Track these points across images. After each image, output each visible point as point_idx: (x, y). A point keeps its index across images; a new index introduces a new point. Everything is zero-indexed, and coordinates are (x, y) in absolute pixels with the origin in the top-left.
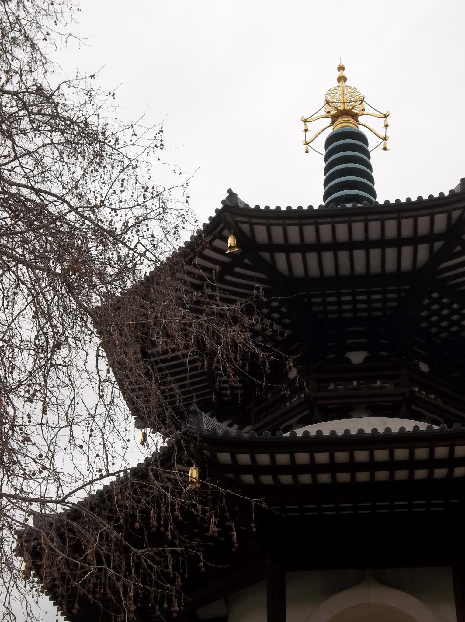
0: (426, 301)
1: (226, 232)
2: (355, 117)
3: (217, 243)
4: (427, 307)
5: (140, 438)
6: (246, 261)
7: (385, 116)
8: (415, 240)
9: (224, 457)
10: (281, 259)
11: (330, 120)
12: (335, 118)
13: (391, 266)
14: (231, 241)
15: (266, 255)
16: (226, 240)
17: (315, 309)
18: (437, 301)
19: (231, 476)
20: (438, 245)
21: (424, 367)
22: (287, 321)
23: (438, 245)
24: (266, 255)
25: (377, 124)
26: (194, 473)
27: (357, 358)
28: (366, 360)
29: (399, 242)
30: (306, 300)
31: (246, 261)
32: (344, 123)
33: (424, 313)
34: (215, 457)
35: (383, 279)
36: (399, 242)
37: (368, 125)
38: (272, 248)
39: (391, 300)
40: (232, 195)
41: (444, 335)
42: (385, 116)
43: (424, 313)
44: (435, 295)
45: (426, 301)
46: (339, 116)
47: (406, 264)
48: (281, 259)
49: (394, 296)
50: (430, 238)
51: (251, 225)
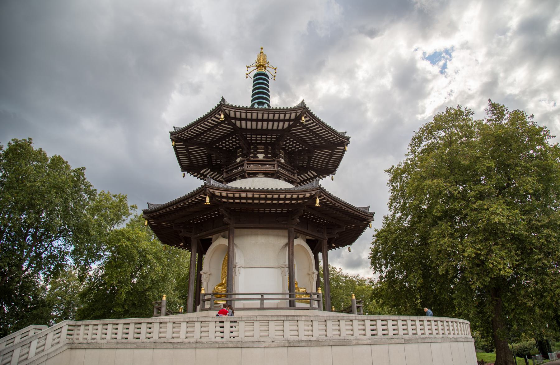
1: (220, 112)
2: (265, 67)
3: (217, 116)
4: (285, 141)
5: (183, 175)
8: (284, 121)
9: (218, 193)
11: (256, 68)
12: (258, 67)
13: (275, 128)
14: (222, 116)
15: (233, 121)
16: (220, 115)
18: (289, 139)
20: (291, 123)
21: (283, 161)
22: (238, 142)
23: (291, 123)
24: (233, 121)
25: (273, 71)
26: (208, 199)
28: (264, 157)
29: (279, 121)
32: (262, 70)
36: (279, 121)
37: (269, 71)
38: (235, 118)
40: (223, 100)
48: (238, 123)
50: (289, 120)
51: (229, 111)
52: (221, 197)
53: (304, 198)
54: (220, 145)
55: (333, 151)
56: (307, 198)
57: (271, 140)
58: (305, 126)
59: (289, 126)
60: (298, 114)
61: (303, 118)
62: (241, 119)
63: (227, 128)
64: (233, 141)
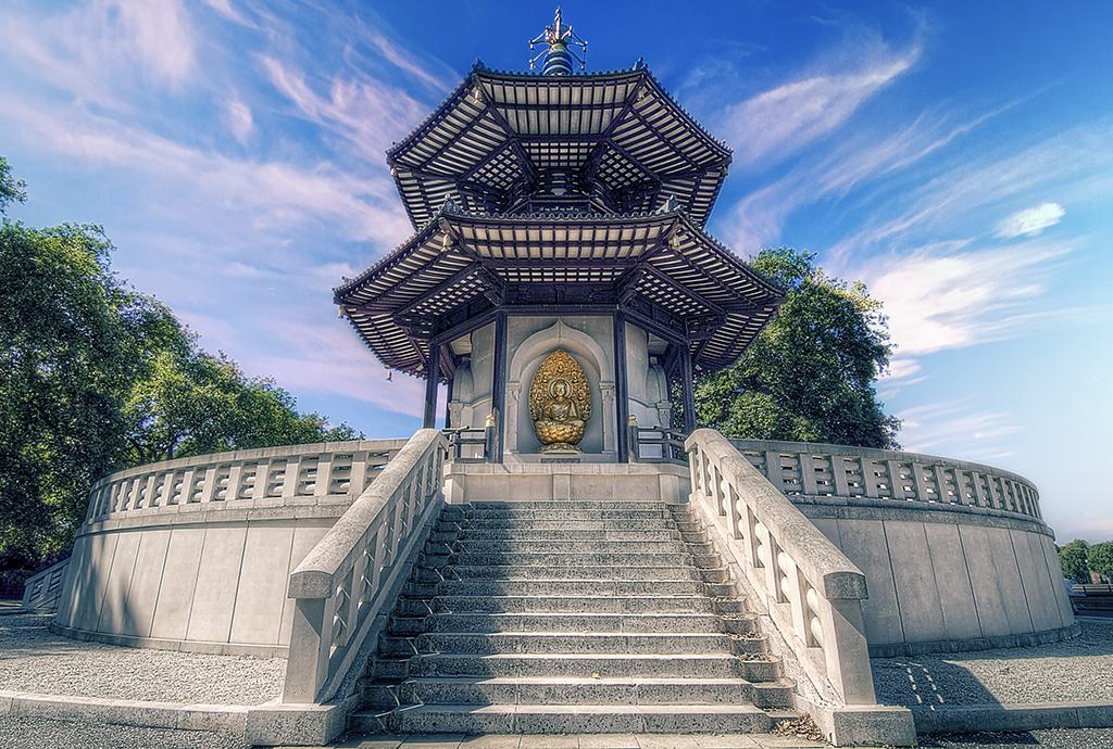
0: (605, 157)
4: (605, 162)
6: (489, 115)
8: (602, 106)
9: (467, 232)
10: (511, 112)
18: (612, 157)
19: (472, 247)
20: (617, 111)
23: (617, 111)
26: (445, 240)
27: (559, 192)
31: (489, 115)
33: (603, 166)
34: (461, 230)
35: (579, 137)
38: (505, 105)
43: (603, 166)
44: (611, 152)
45: (605, 157)
47: (595, 129)
49: (585, 151)
52: (476, 241)
53: (644, 242)
54: (483, 175)
56: (652, 240)
57: (578, 161)
58: (643, 121)
59: (617, 121)
60: (631, 86)
61: (641, 95)
62: (516, 106)
64: (507, 166)
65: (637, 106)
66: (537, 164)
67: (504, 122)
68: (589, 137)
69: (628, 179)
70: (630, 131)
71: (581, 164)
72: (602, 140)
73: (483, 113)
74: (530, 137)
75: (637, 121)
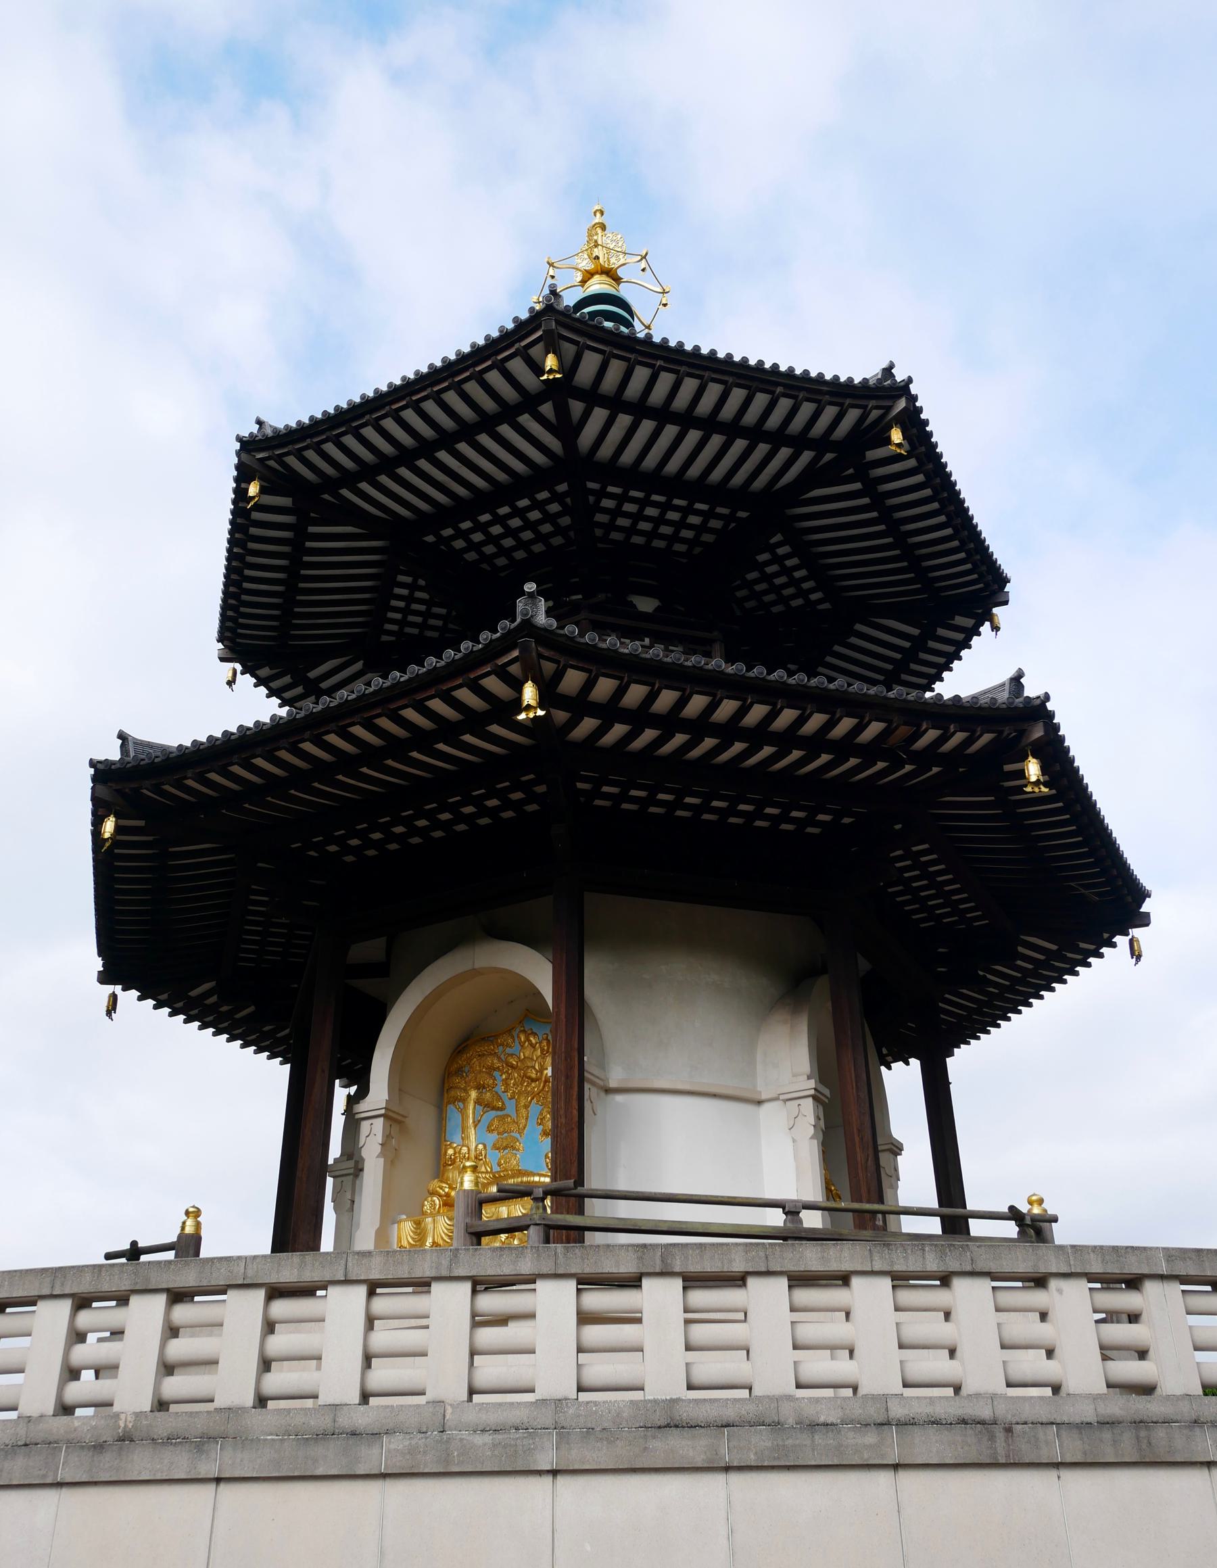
2: (618, 280)
7: (664, 292)
8: (800, 442)
17: (601, 518)
23: (829, 456)
24: (577, 407)
27: (646, 605)
28: (656, 610)
30: (591, 499)
31: (547, 409)
35: (720, 493)
39: (712, 531)
41: (751, 604)
42: (664, 292)
46: (597, 273)
50: (823, 444)
55: (929, 633)
59: (812, 477)
63: (530, 443)
65: (873, 455)
66: (599, 532)
67: (567, 430)
68: (740, 497)
69: (784, 600)
70: (833, 507)
71: (697, 550)
72: (771, 508)
73: (529, 402)
74: (611, 471)
75: (857, 486)
